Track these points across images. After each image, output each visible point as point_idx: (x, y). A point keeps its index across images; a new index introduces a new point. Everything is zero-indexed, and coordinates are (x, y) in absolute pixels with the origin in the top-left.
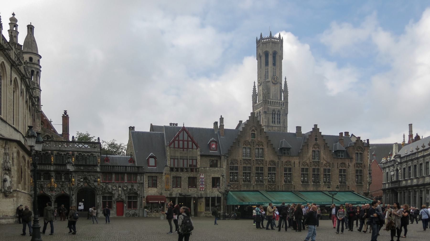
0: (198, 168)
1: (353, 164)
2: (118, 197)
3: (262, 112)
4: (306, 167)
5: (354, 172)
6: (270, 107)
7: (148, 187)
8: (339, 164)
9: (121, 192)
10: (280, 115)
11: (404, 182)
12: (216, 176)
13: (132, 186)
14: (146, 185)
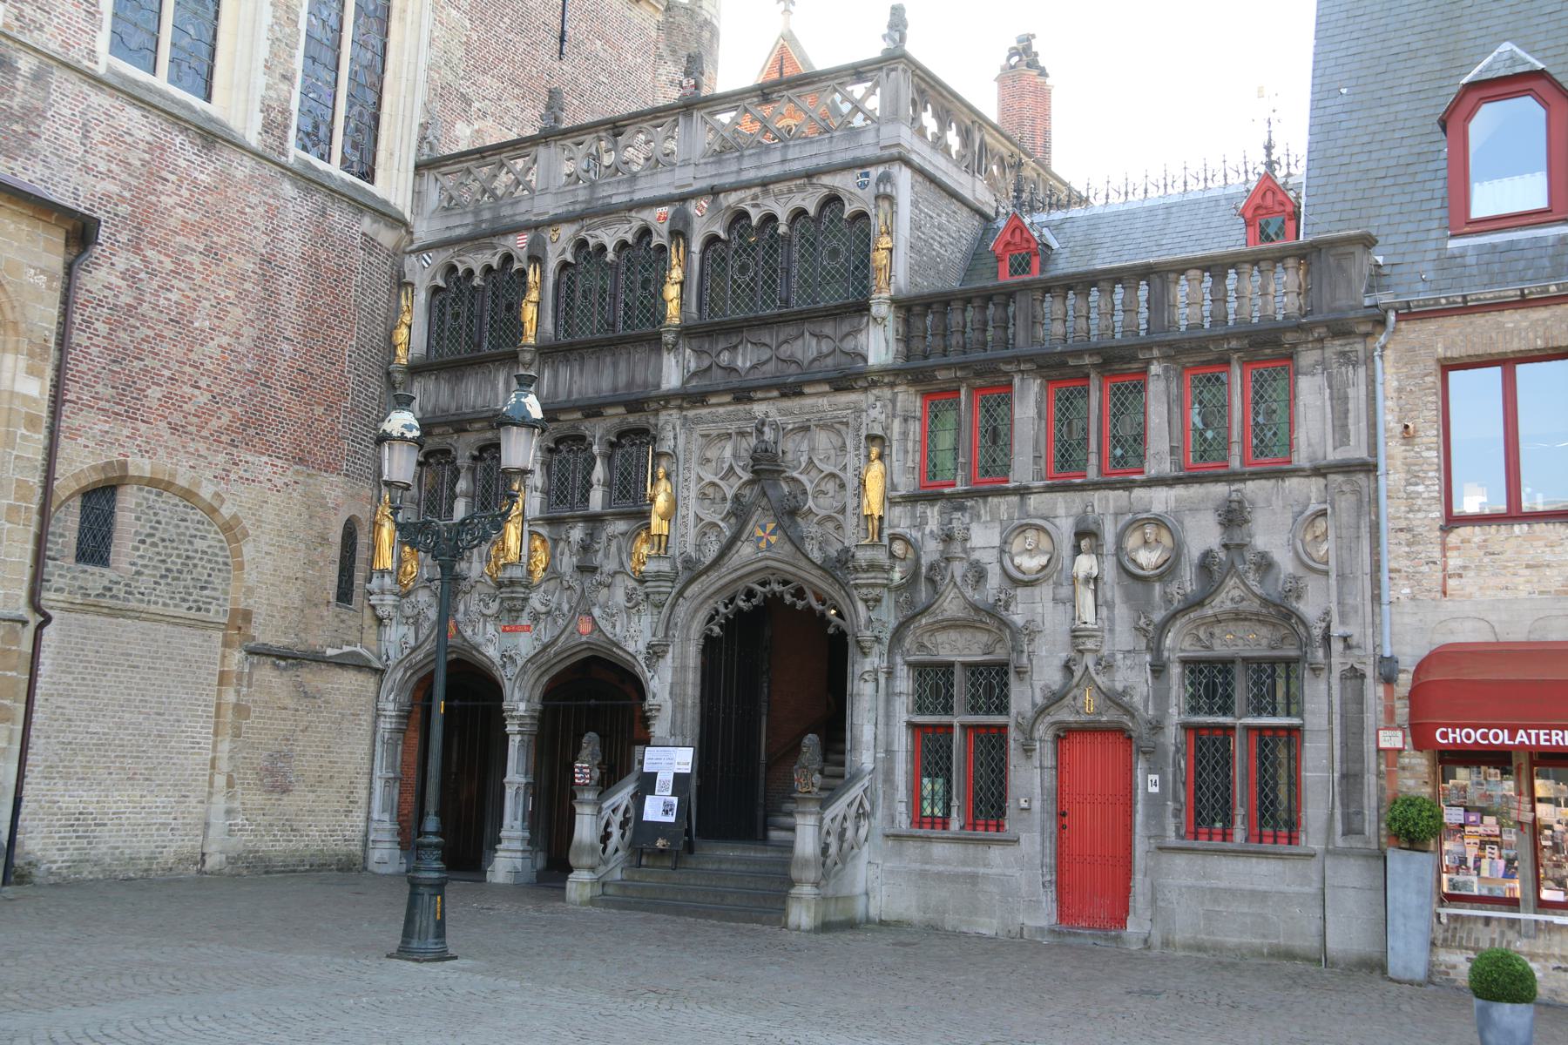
13: (1233, 517)
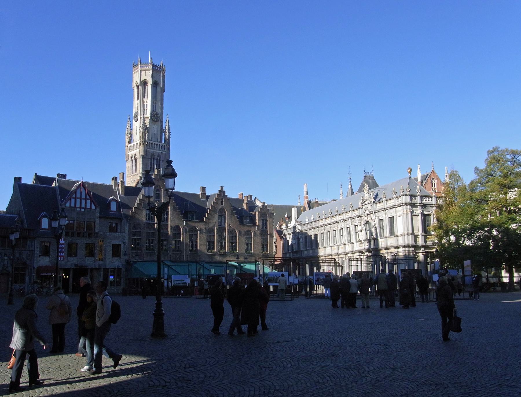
0: (97, 233)
2: (3, 268)
3: (138, 155)
7: (40, 256)
9: (7, 262)
10: (160, 160)
11: (306, 252)
12: (117, 242)
13: (20, 254)
14: (37, 252)
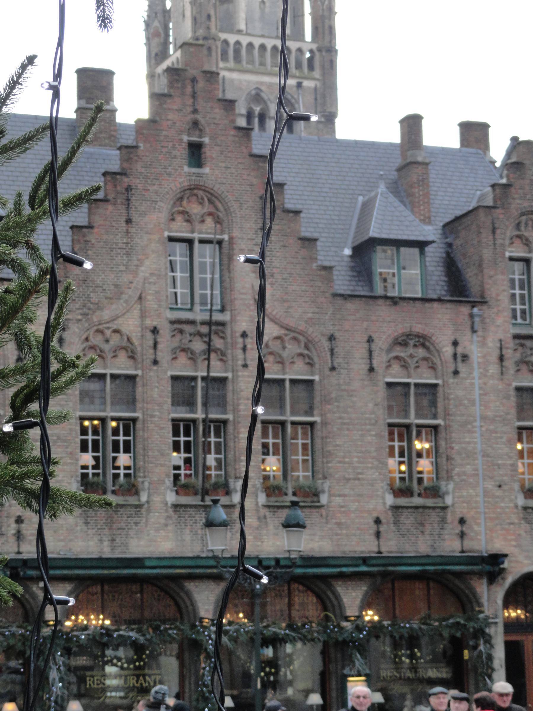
1: (492, 344)
4: (121, 366)
5: (504, 406)
6: (235, 76)
8: (382, 342)
